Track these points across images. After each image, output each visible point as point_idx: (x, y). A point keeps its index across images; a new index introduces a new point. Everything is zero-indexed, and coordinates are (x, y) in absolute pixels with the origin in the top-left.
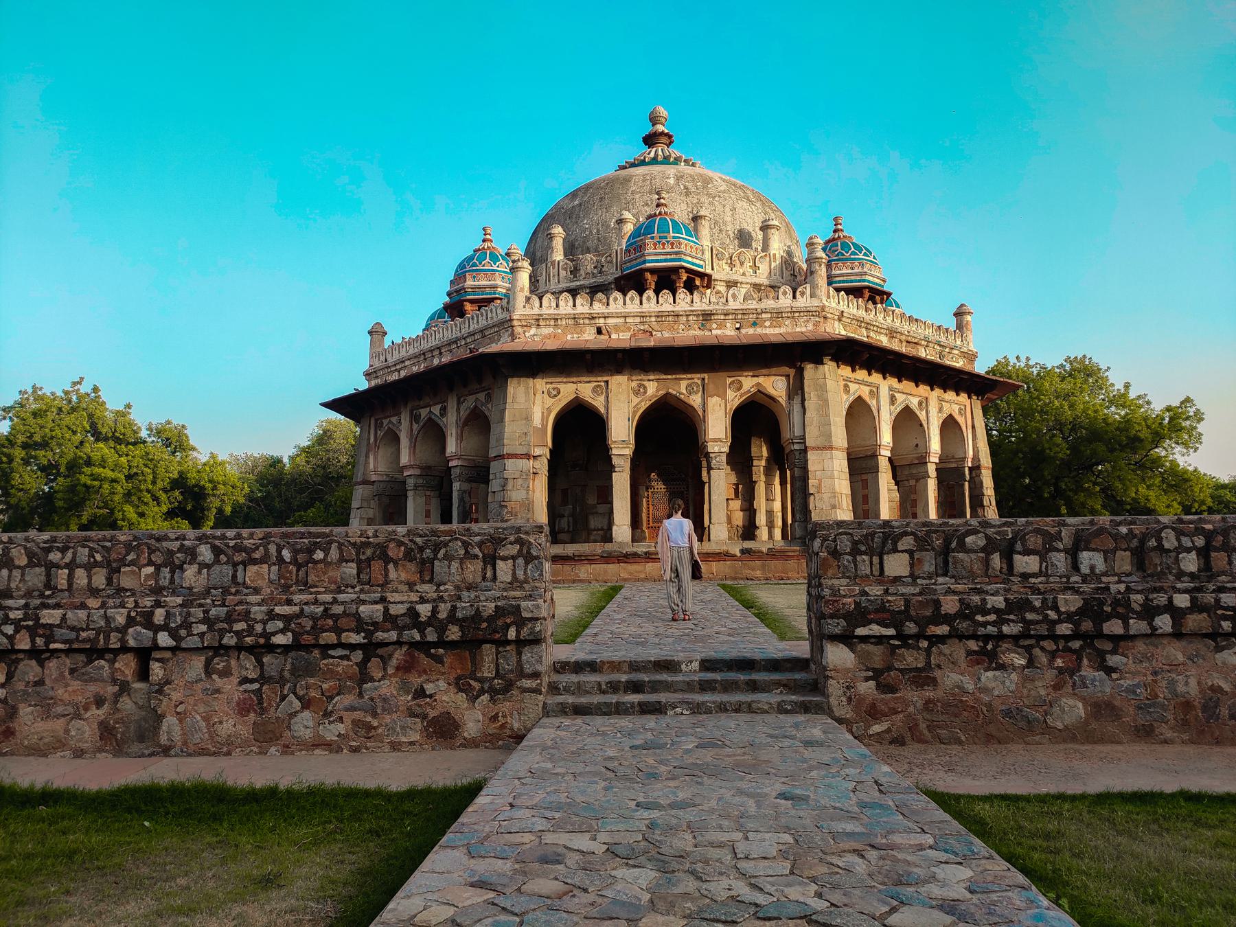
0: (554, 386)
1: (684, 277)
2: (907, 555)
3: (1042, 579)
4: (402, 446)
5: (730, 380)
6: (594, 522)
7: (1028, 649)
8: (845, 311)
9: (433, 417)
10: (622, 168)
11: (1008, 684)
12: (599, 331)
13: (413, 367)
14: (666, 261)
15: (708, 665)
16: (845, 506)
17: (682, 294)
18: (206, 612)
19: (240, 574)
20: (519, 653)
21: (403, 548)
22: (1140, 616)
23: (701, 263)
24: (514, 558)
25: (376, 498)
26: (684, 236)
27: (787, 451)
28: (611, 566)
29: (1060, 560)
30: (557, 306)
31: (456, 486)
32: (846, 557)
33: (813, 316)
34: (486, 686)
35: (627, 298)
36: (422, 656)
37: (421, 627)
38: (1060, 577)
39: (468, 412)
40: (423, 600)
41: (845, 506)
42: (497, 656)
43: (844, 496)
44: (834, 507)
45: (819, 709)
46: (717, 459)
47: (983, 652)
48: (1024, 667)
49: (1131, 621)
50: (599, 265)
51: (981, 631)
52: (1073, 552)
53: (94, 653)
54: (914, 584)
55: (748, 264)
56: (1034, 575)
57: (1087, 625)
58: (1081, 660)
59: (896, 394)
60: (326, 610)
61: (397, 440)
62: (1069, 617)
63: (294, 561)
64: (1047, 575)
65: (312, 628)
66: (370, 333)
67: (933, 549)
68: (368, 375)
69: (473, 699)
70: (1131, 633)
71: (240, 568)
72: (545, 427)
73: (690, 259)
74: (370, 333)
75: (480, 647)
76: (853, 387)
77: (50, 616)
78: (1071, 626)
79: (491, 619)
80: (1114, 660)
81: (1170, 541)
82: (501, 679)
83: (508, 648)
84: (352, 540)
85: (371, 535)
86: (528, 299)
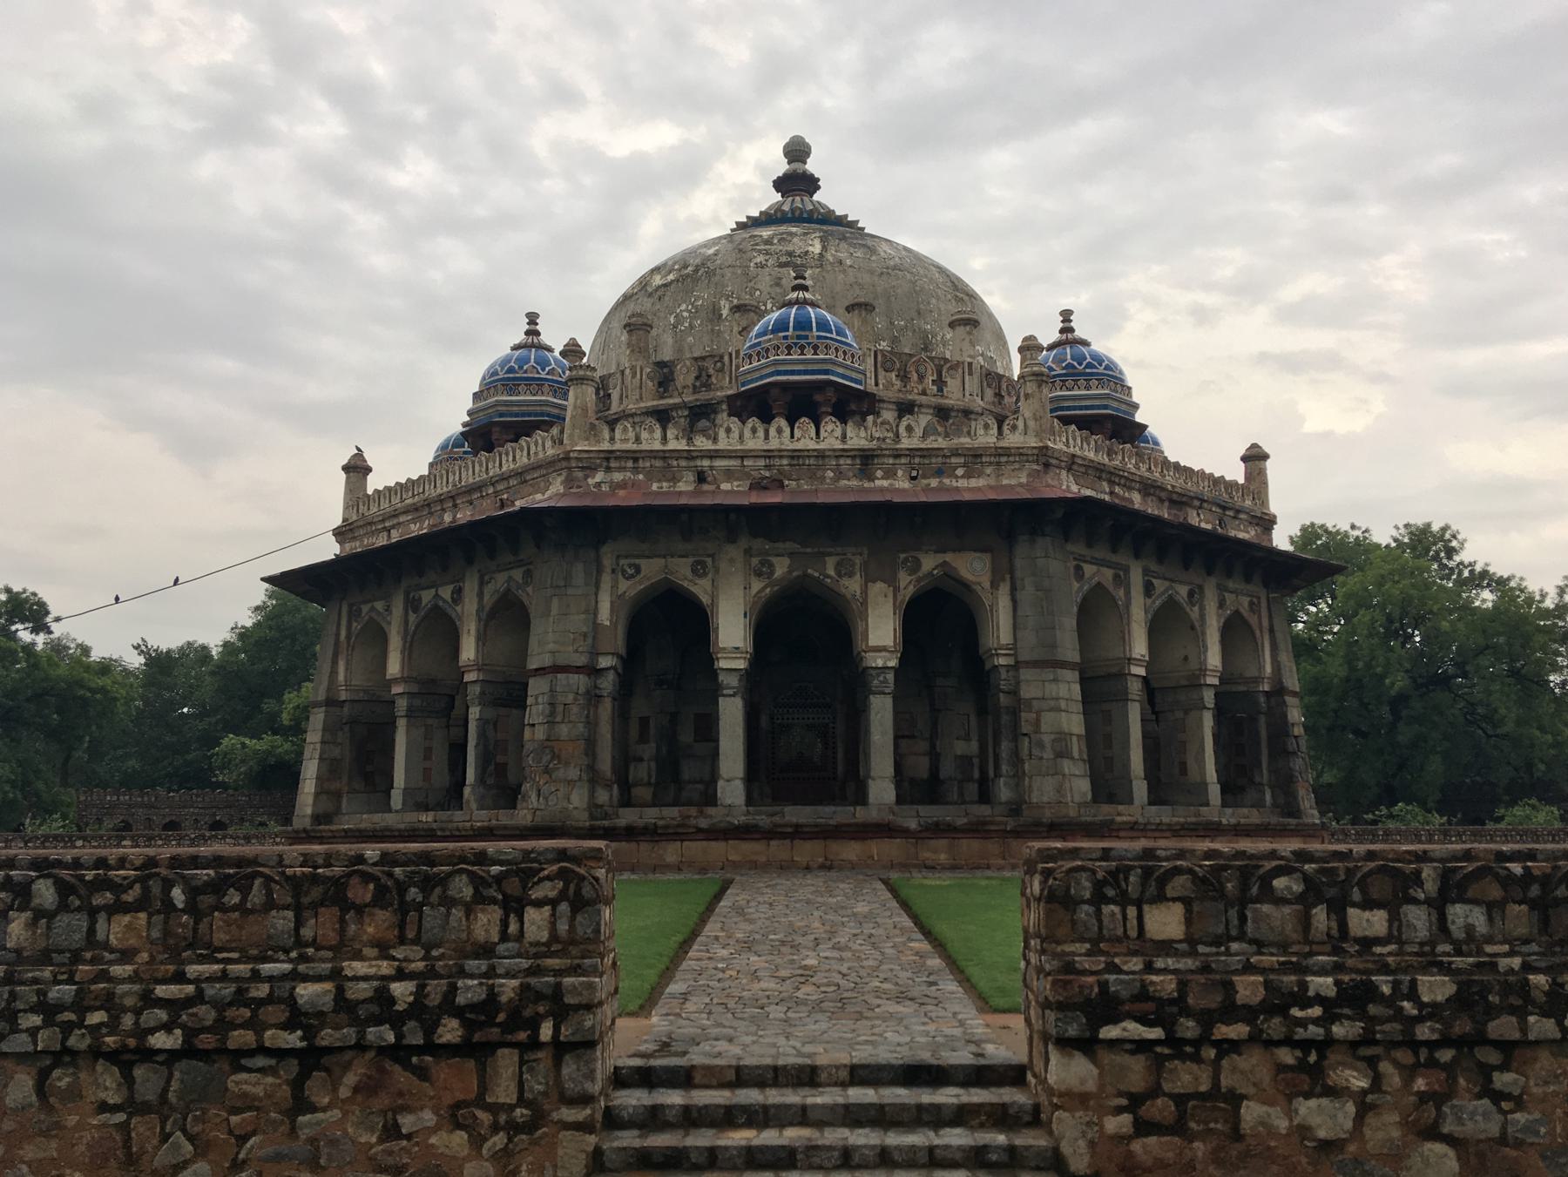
0: (632, 561)
2: (1178, 909)
3: (1392, 947)
5: (902, 556)
6: (688, 771)
7: (1372, 1062)
8: (1079, 453)
9: (441, 603)
10: (741, 226)
11: (1340, 1115)
12: (701, 478)
13: (412, 526)
14: (806, 372)
15: (860, 1075)
17: (831, 426)
18: (42, 993)
19: (101, 926)
20: (558, 1063)
21: (371, 886)
23: (860, 376)
24: (554, 903)
25: (347, 728)
26: (834, 336)
27: (988, 666)
28: (713, 844)
30: (638, 440)
31: (474, 712)
32: (1086, 907)
33: (1028, 461)
34: (503, 1118)
35: (747, 433)
36: (397, 1068)
37: (397, 1021)
38: (1422, 944)
39: (496, 597)
40: (401, 975)
41: (1076, 754)
42: (520, 1068)
43: (1075, 739)
46: (881, 678)
47: (1302, 1066)
48: (1364, 1092)
49: (1532, 1019)
50: (704, 374)
51: (1300, 1033)
52: (1438, 905)
54: (1193, 953)
55: (930, 378)
56: (1377, 941)
57: (1463, 1026)
58: (1455, 1081)
59: (1154, 581)
60: (239, 991)
61: (382, 639)
62: (1432, 1011)
63: (192, 908)
64: (1401, 943)
65: (216, 1021)
66: (347, 468)
67: (1222, 894)
68: (339, 534)
69: (477, 1142)
70: (1531, 1037)
71: (102, 919)
72: (614, 624)
73: (841, 370)
74: (347, 468)
75: (493, 1053)
76: (1089, 569)
78: (1438, 1026)
80: (1502, 1080)
82: (526, 1107)
83: (540, 1055)
84: (289, 871)
85: (320, 861)
86: (593, 427)
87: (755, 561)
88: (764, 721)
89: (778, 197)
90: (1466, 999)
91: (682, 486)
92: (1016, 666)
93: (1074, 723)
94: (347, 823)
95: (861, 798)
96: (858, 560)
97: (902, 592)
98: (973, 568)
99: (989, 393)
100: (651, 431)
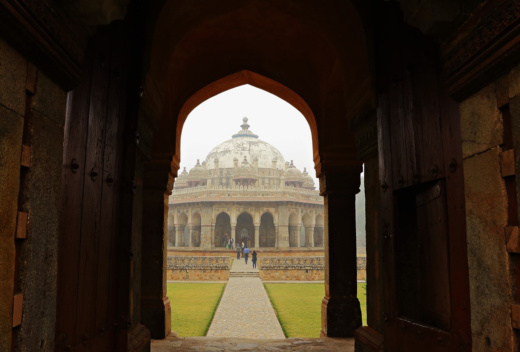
1: (250, 180)
4: (175, 219)
10: (234, 136)
16: (287, 240)
22: (291, 268)
31: (191, 231)
35: (236, 188)
40: (217, 265)
41: (287, 240)
45: (259, 277)
53: (183, 269)
57: (286, 268)
76: (291, 210)
77: (177, 265)
79: (225, 267)
86: (211, 186)
87: (237, 209)
88: (238, 232)
89: (241, 129)
91: (225, 196)
93: (287, 235)
97: (260, 214)
98: (272, 210)
99: (278, 174)
100: (221, 187)
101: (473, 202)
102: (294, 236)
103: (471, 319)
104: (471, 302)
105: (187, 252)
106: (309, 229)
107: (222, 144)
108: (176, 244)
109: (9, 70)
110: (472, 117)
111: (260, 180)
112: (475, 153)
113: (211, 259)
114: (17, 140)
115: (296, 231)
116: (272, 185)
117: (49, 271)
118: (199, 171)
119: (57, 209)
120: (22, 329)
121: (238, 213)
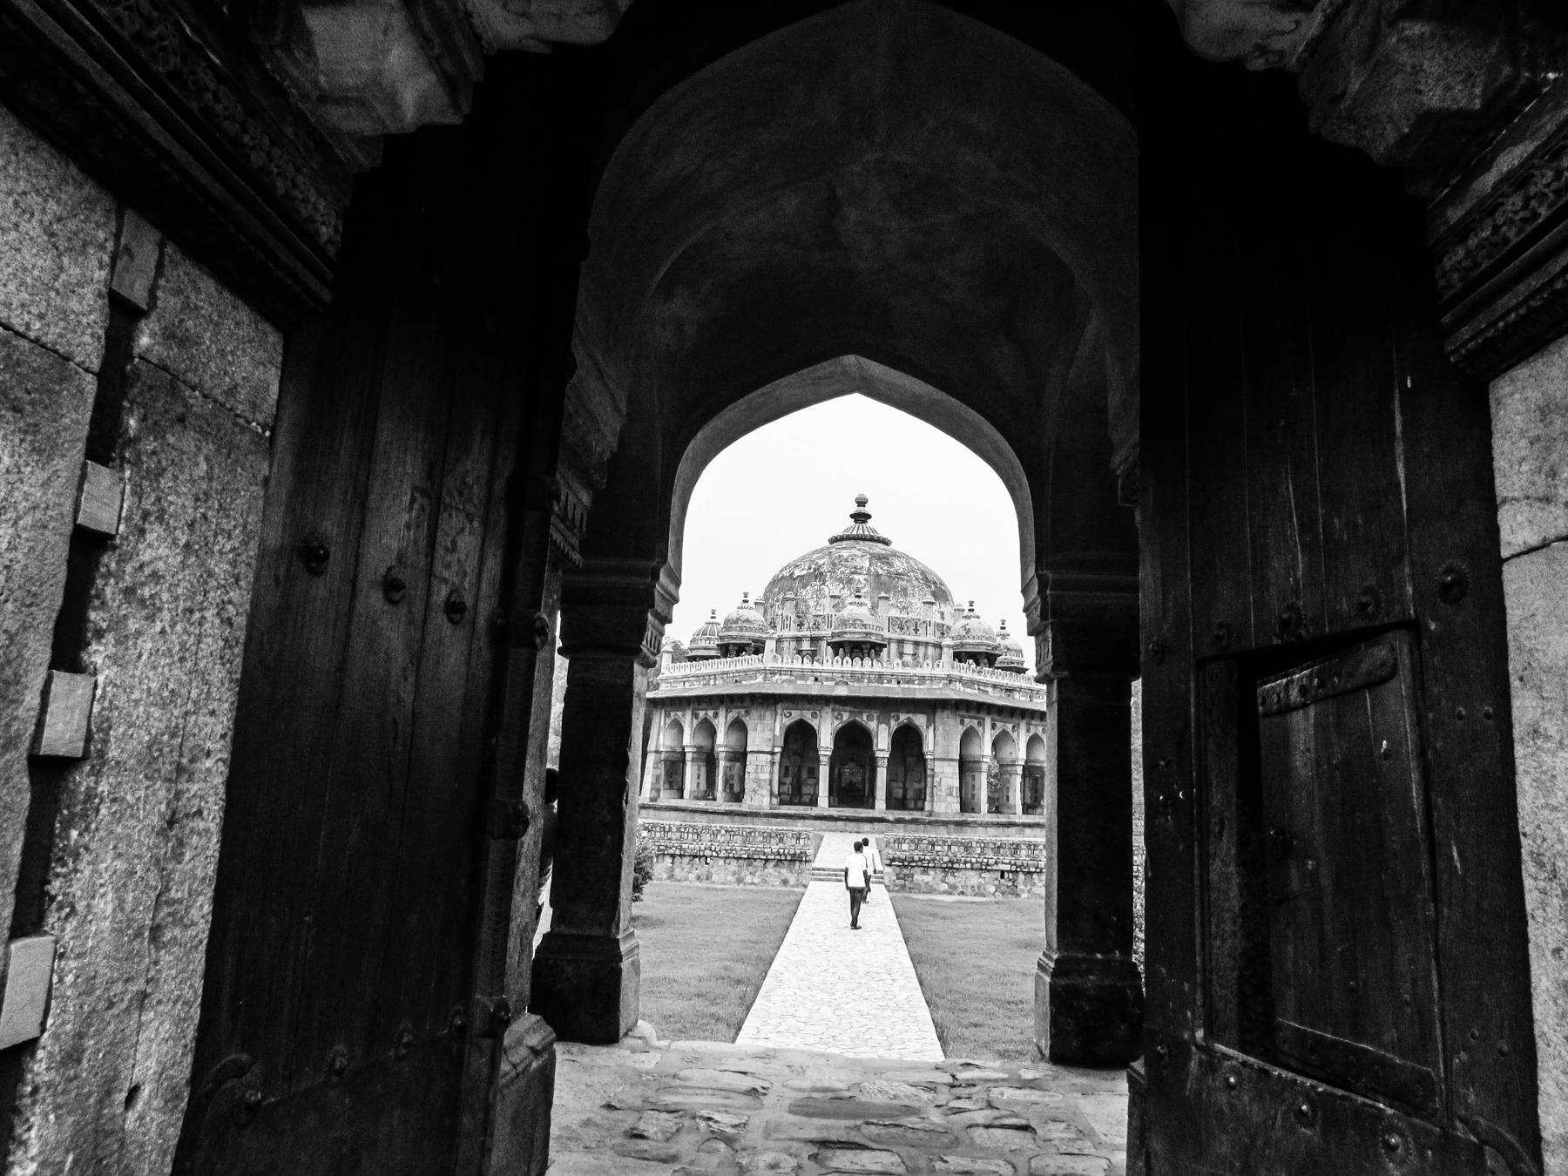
1: (869, 646)
6: (806, 790)
10: (834, 540)
12: (816, 679)
29: (946, 848)
31: (722, 764)
44: (948, 795)
45: (881, 883)
53: (695, 857)
57: (950, 865)
76: (967, 721)
77: (685, 846)
81: (974, 845)
87: (836, 714)
88: (836, 771)
90: (950, 861)
92: (934, 759)
93: (957, 784)
94: (660, 803)
95: (873, 807)
96: (875, 715)
98: (920, 720)
99: (938, 634)
101: (1543, 698)
102: (973, 786)
103: (1540, 1092)
104: (1537, 1032)
105: (711, 813)
106: (1009, 769)
107: (803, 559)
108: (686, 794)
109: (32, 215)
110: (1541, 421)
111: (894, 646)
112: (1553, 537)
113: (768, 836)
114: (60, 441)
115: (976, 774)
116: (921, 660)
117: (180, 863)
118: (747, 621)
119: (229, 672)
120: (40, 1054)
121: (838, 724)
